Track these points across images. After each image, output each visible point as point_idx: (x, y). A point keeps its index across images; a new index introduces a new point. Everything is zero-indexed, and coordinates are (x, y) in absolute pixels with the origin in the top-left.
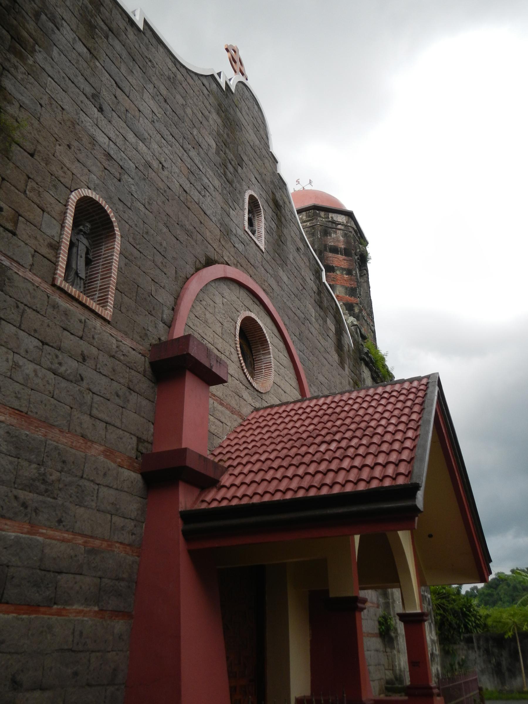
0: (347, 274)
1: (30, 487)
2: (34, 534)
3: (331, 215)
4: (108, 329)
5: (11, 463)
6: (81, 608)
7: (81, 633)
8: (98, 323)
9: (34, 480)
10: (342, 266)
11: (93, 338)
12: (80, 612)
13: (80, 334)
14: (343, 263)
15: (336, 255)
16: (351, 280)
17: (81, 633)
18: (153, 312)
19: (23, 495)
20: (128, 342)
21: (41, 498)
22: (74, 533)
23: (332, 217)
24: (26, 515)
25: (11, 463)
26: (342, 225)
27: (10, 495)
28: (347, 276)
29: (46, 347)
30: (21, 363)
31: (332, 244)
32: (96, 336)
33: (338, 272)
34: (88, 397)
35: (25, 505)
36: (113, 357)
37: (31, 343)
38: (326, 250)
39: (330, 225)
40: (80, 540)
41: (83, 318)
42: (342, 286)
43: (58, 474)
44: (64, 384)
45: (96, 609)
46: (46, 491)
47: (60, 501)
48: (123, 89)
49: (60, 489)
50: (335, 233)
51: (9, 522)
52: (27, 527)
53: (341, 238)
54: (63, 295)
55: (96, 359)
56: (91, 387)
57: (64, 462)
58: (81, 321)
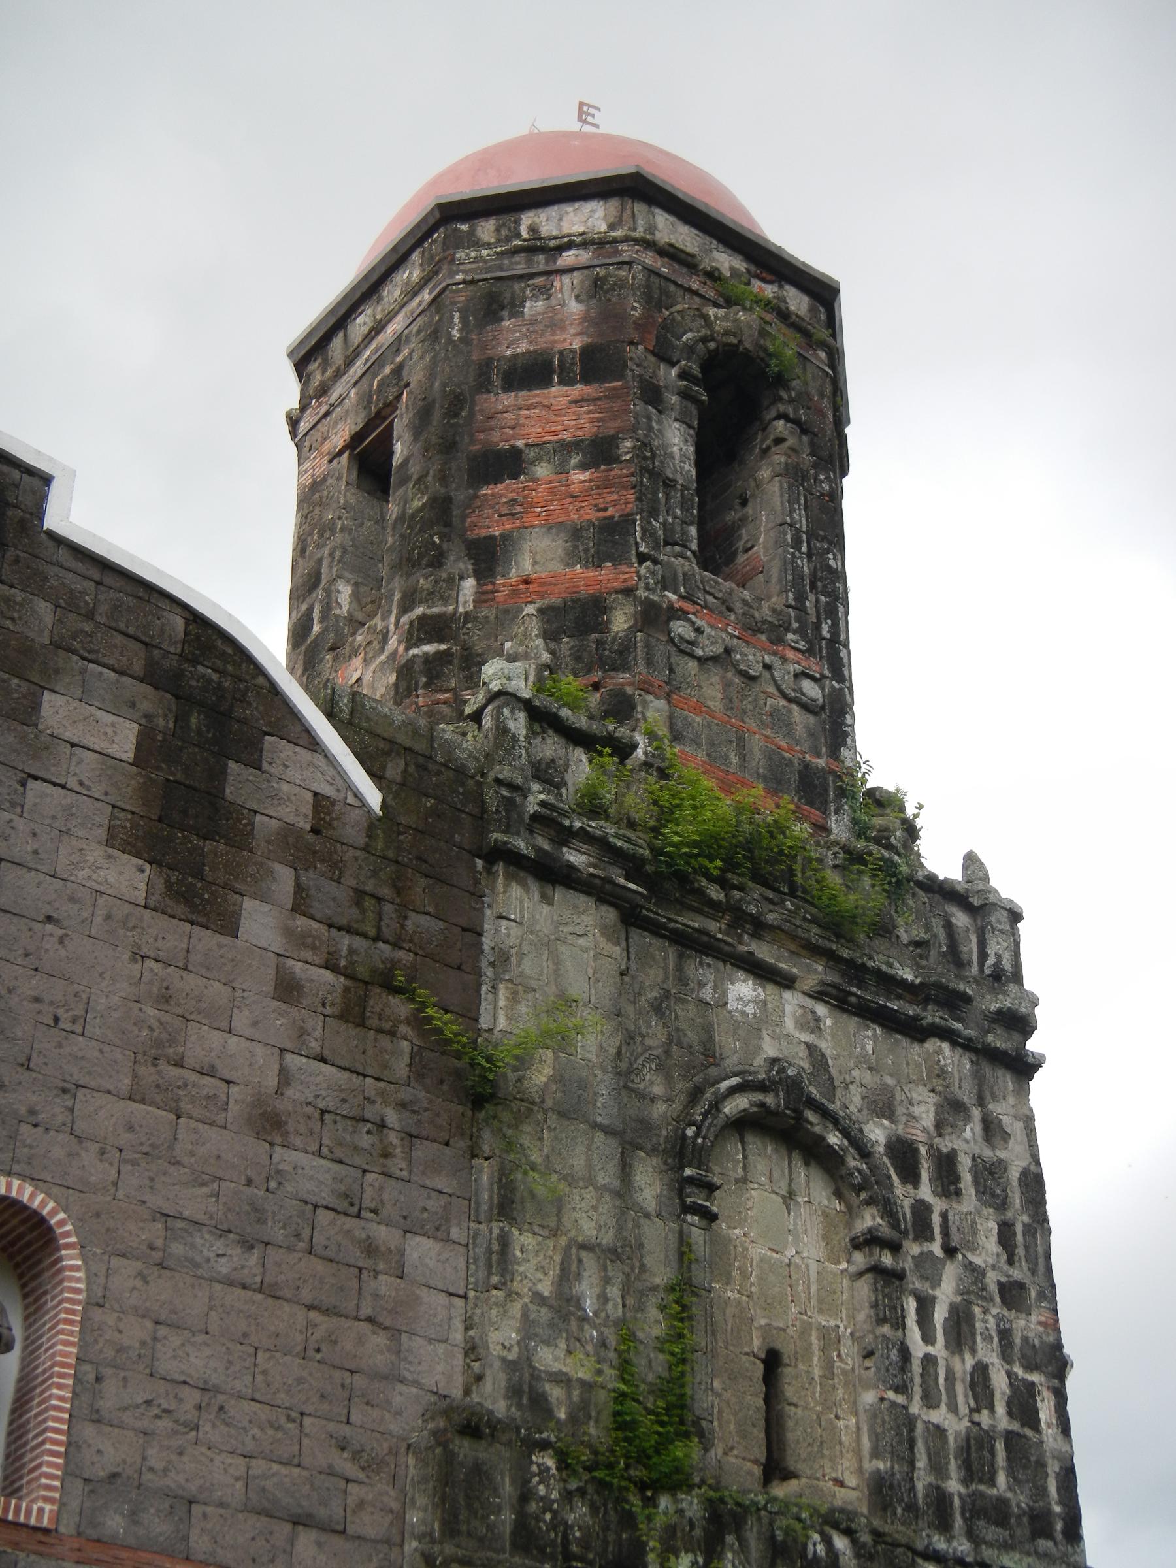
0: (583, 467)
3: (527, 220)
10: (565, 436)
14: (569, 421)
15: (537, 395)
16: (605, 485)
23: (533, 229)
26: (584, 245)
28: (586, 475)
31: (523, 347)
33: (542, 471)
38: (483, 385)
39: (520, 266)
42: (553, 527)
50: (545, 291)
53: (575, 308)
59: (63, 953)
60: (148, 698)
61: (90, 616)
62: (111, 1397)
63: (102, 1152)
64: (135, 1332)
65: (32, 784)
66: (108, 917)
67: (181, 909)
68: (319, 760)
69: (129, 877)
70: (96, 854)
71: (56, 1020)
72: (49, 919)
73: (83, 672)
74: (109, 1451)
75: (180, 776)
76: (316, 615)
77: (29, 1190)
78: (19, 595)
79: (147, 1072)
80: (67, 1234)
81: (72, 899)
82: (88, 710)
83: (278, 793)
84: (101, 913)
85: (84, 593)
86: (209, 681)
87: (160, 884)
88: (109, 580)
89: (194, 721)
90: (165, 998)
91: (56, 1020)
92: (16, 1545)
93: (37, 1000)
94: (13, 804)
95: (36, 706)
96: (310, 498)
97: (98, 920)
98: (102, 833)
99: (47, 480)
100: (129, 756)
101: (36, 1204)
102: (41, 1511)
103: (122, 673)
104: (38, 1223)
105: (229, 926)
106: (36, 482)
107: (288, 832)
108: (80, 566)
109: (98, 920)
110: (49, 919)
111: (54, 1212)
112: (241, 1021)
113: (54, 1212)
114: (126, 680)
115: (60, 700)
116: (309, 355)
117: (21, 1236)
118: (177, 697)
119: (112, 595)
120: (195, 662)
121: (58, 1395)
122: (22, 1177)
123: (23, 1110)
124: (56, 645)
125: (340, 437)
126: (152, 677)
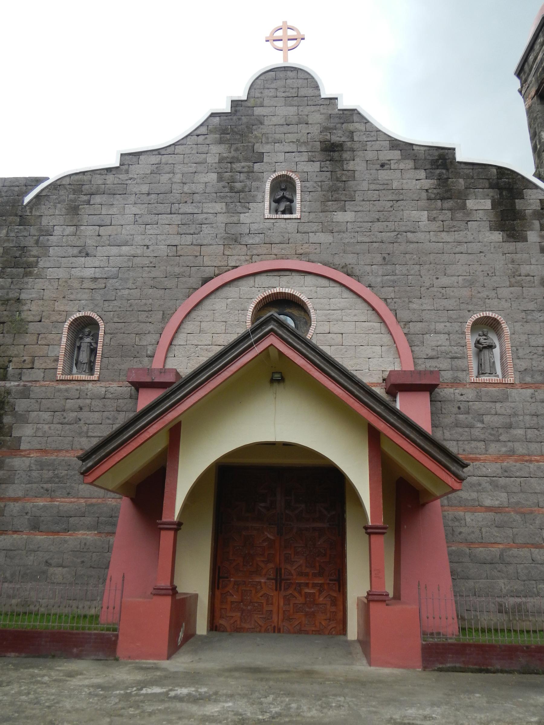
1: (50, 481)
2: (54, 502)
4: (98, 384)
5: (38, 473)
6: (85, 532)
7: (85, 544)
8: (90, 385)
9: (52, 478)
11: (87, 395)
12: (85, 534)
13: (77, 397)
17: (85, 544)
18: (138, 355)
19: (45, 486)
20: (115, 385)
21: (56, 485)
22: (78, 498)
24: (48, 494)
25: (38, 473)
27: (39, 487)
29: (56, 413)
30: (41, 427)
32: (89, 393)
34: (85, 428)
35: (47, 490)
36: (104, 398)
37: (46, 416)
40: (82, 501)
41: (78, 387)
43: (66, 472)
44: (68, 427)
45: (96, 532)
46: (60, 481)
47: (68, 484)
48: (105, 224)
49: (68, 479)
51: (39, 499)
52: (49, 499)
54: (64, 382)
55: (90, 406)
56: (88, 422)
57: (69, 465)
58: (77, 390)
59: (486, 259)
60: (491, 192)
61: (473, 178)
62: (521, 353)
63: (506, 300)
64: (524, 338)
65: (469, 223)
66: (495, 247)
67: (512, 240)
68: (539, 191)
69: (497, 236)
70: (488, 234)
71: (488, 274)
72: (481, 252)
73: (474, 192)
74: (523, 365)
75: (504, 208)
76: (538, 143)
77: (491, 313)
78: (454, 180)
79: (513, 280)
80: (502, 321)
81: (485, 246)
82: (477, 201)
83: (531, 203)
84: (493, 247)
85: (470, 173)
86: (506, 182)
87: (505, 236)
88: (475, 167)
89: (504, 193)
90: (513, 261)
91: (488, 274)
92: (507, 388)
93: (482, 271)
94: (466, 229)
95: (465, 204)
96: (530, 111)
97: (492, 249)
98: (488, 228)
99: (454, 149)
100: (490, 208)
101: (493, 316)
102: (510, 380)
103: (483, 189)
104: (495, 320)
105: (525, 239)
106: (451, 151)
107: (535, 213)
108: (467, 167)
109: (492, 249)
110: (481, 252)
111: (498, 317)
112: (533, 261)
113: (498, 317)
114: (485, 190)
115: (470, 201)
116: (520, 72)
117: (492, 323)
118: (499, 189)
119: (477, 170)
120: (501, 179)
121: (509, 355)
122: (489, 311)
123: (485, 296)
124: (466, 188)
125: (533, 93)
126: (491, 187)
